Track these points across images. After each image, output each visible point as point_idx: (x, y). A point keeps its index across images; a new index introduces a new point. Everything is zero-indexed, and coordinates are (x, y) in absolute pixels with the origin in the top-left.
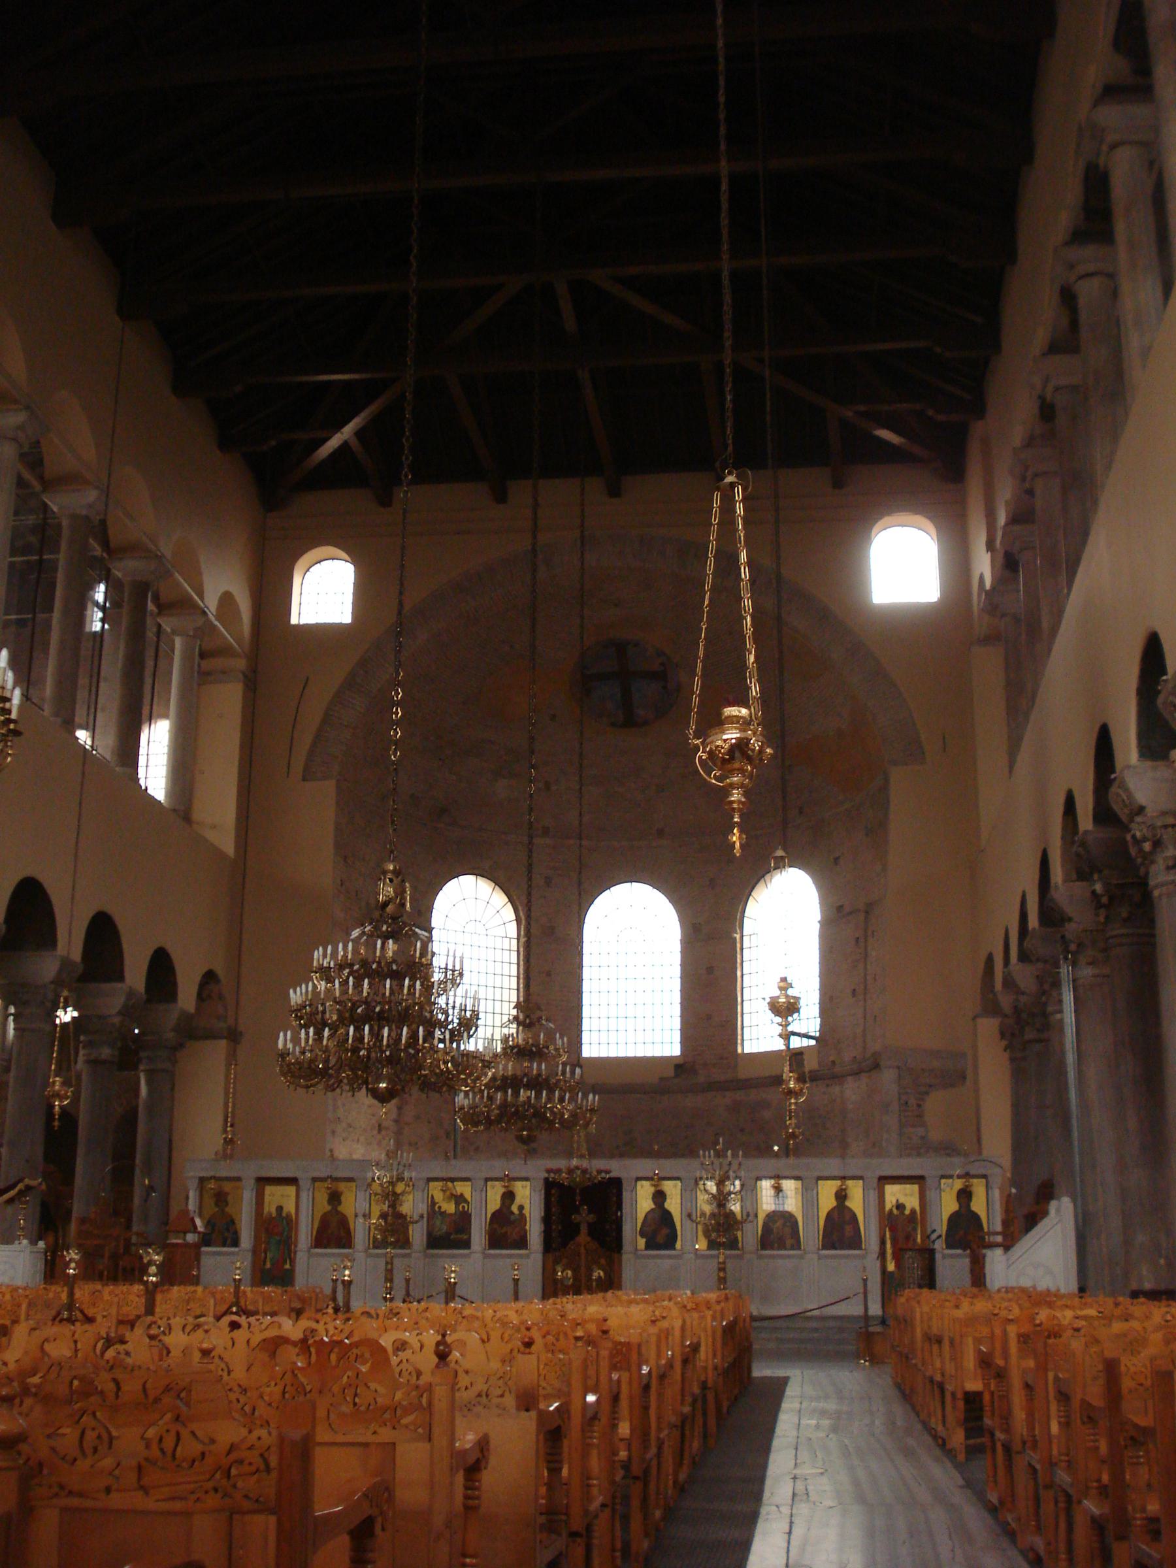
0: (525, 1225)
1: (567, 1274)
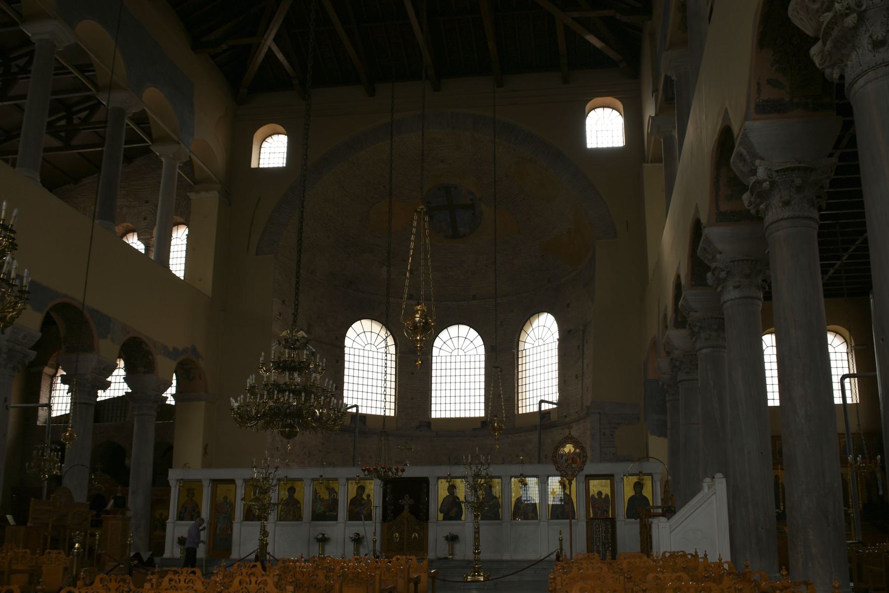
0: (371, 506)
1: (396, 535)
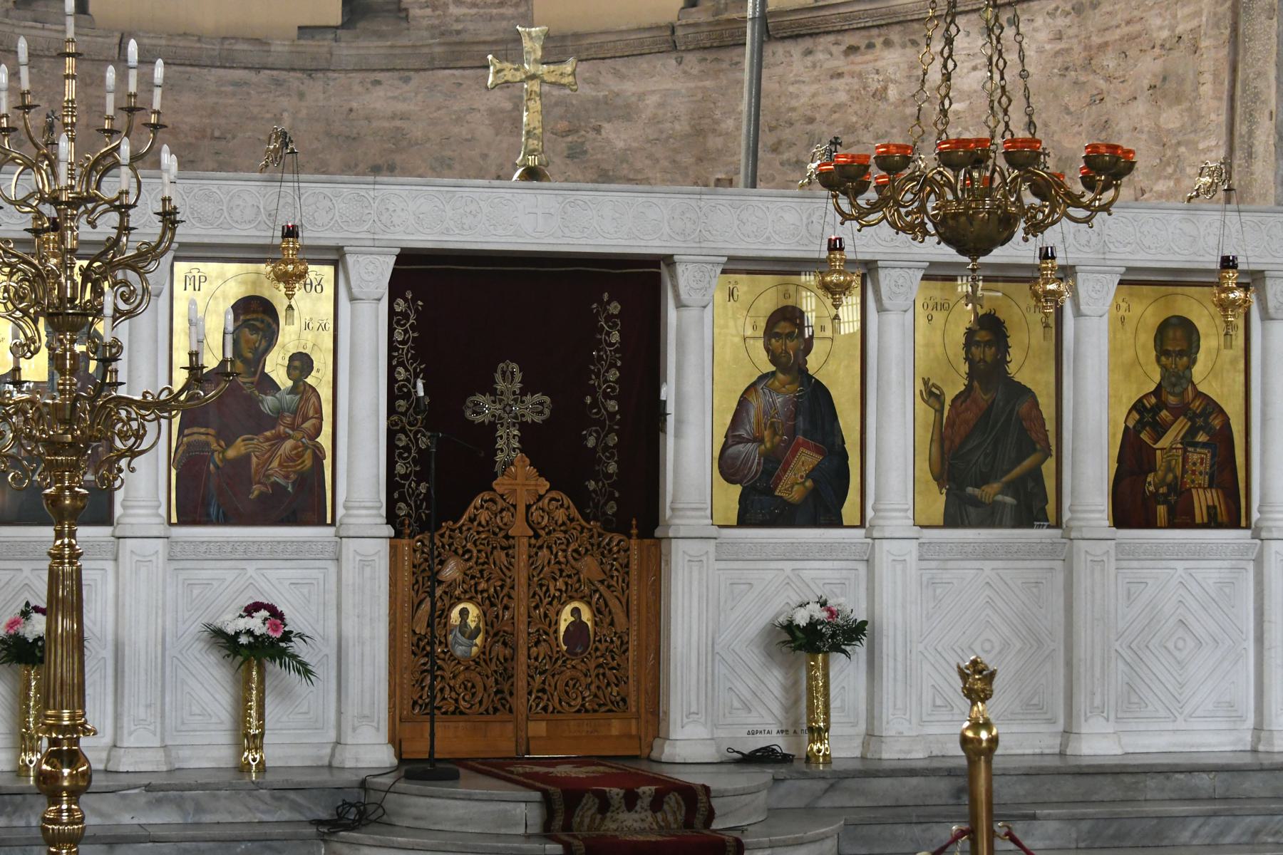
0: (318, 431)
1: (464, 613)
